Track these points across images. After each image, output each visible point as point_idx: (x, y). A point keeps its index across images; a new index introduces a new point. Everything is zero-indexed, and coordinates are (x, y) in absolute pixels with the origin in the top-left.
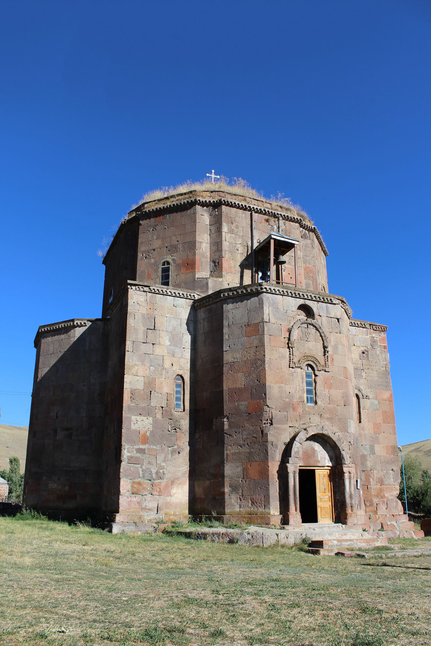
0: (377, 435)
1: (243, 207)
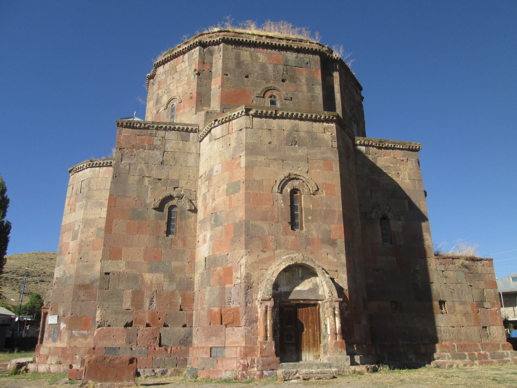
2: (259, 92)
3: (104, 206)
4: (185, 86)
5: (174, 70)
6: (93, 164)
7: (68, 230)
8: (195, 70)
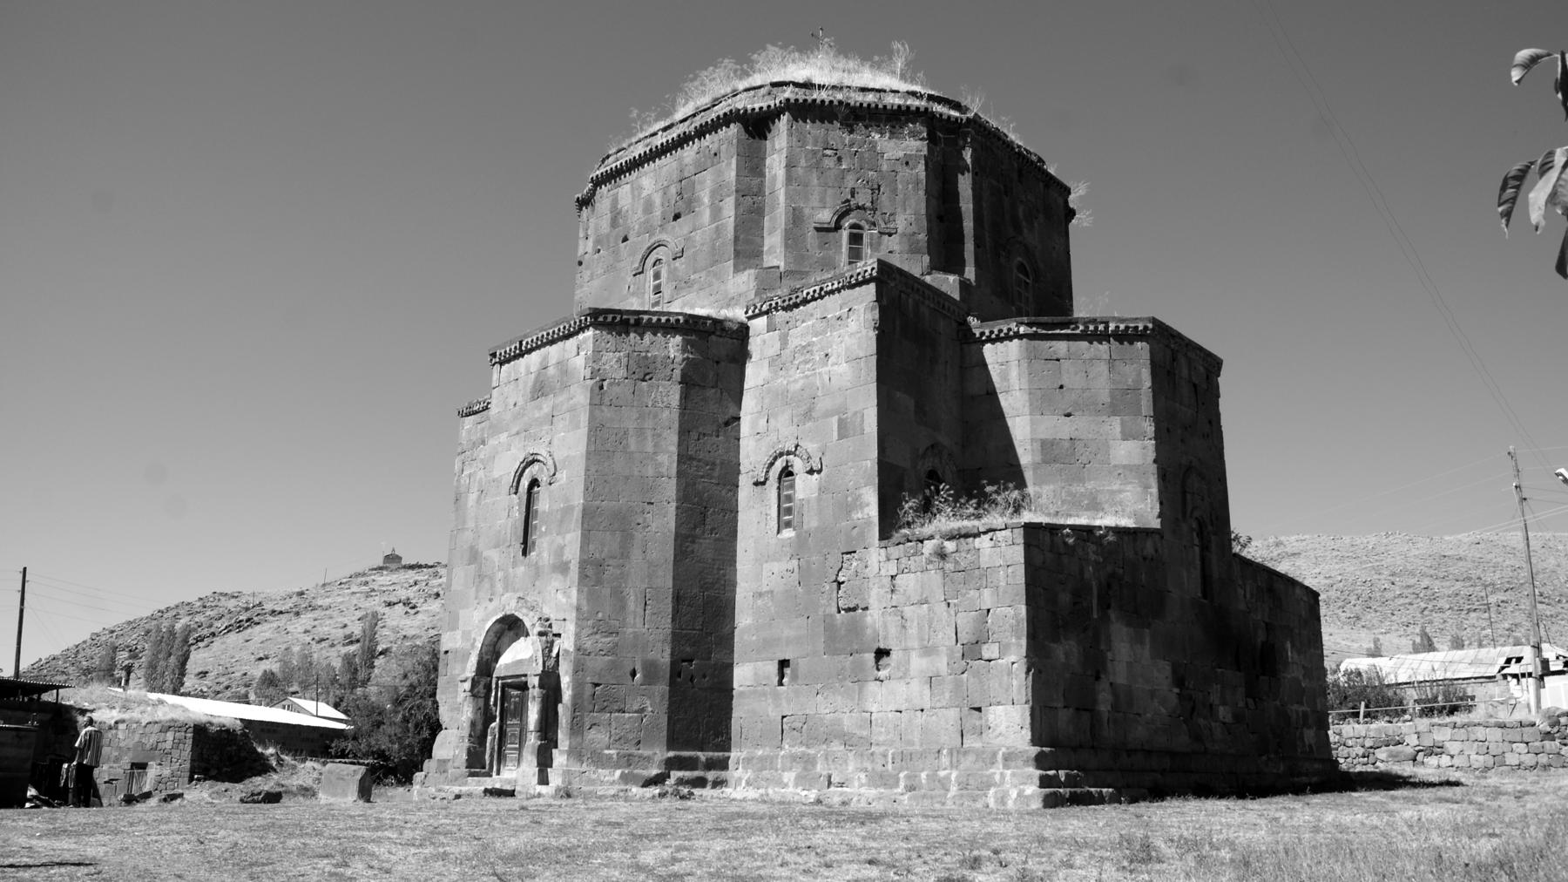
2: (637, 265)
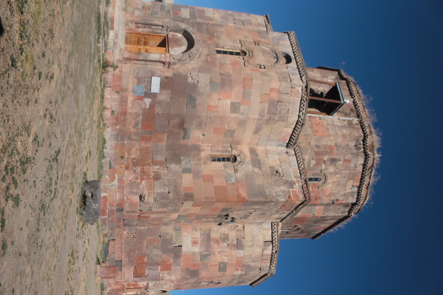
0: (202, 178)
1: (352, 93)
3: (254, 134)
4: (330, 191)
5: (351, 177)
6: (299, 125)
7: (244, 93)
8: (338, 200)
